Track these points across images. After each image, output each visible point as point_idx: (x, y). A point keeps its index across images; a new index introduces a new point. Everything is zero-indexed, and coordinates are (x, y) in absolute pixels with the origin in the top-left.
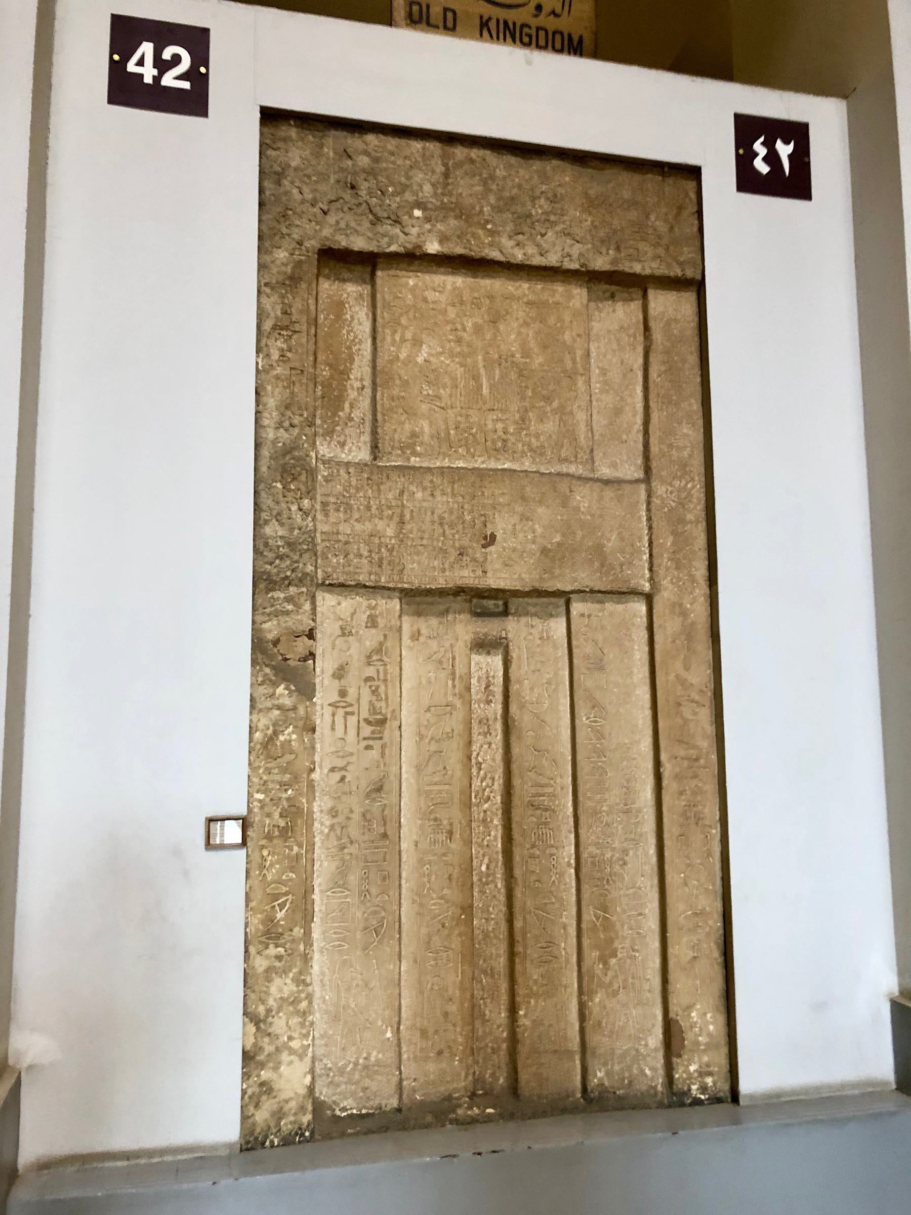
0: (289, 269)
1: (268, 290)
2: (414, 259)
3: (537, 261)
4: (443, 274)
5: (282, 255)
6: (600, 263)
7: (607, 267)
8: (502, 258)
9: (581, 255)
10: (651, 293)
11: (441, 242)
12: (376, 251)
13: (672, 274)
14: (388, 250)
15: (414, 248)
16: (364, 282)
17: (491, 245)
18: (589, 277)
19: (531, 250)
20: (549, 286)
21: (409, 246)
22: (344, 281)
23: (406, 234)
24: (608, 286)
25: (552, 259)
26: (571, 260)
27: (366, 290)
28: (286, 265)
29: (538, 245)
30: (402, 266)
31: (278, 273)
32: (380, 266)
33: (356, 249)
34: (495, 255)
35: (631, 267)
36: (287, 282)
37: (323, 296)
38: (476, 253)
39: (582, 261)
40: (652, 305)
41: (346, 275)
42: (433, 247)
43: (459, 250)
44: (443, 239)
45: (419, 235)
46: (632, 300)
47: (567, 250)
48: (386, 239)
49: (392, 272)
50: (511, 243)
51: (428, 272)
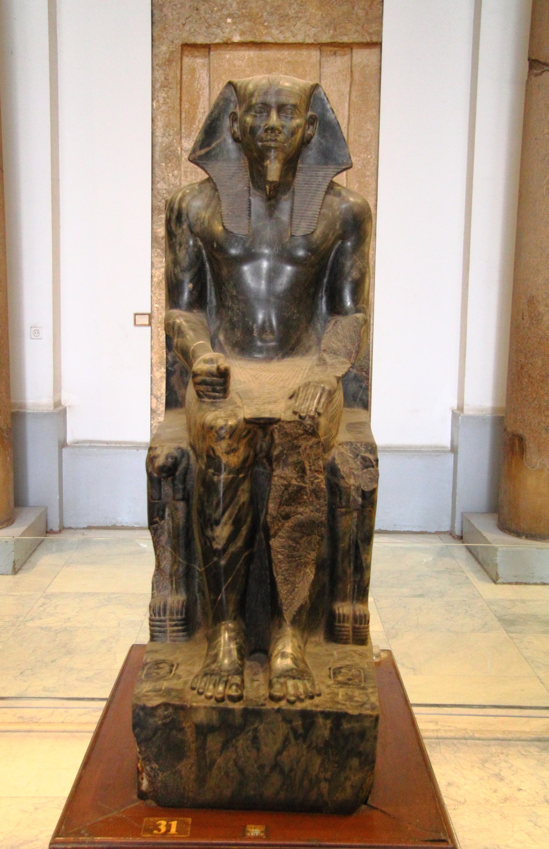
0: (167, 56)
1: (157, 68)
2: (227, 44)
3: (291, 40)
4: (243, 50)
5: (164, 48)
6: (325, 38)
7: (329, 41)
8: (272, 41)
9: (315, 35)
10: (355, 51)
11: (241, 35)
12: (209, 43)
13: (364, 41)
14: (214, 42)
15: (227, 40)
16: (205, 56)
17: (266, 34)
18: (320, 46)
19: (288, 34)
20: (299, 52)
21: (225, 39)
22: (196, 57)
23: (224, 33)
24: (332, 48)
25: (300, 39)
26: (309, 38)
27: (206, 61)
28: (165, 53)
29: (292, 32)
30: (223, 48)
31: (163, 58)
32: (212, 49)
33: (199, 43)
34: (269, 39)
35: (342, 39)
36: (167, 63)
37: (185, 66)
38: (258, 40)
39: (315, 38)
40: (354, 58)
41: (197, 54)
42: (237, 39)
43: (250, 39)
44: (242, 33)
45: (229, 33)
46: (346, 54)
47: (308, 32)
48: (213, 36)
49: (218, 52)
50: (278, 32)
51: (236, 50)
